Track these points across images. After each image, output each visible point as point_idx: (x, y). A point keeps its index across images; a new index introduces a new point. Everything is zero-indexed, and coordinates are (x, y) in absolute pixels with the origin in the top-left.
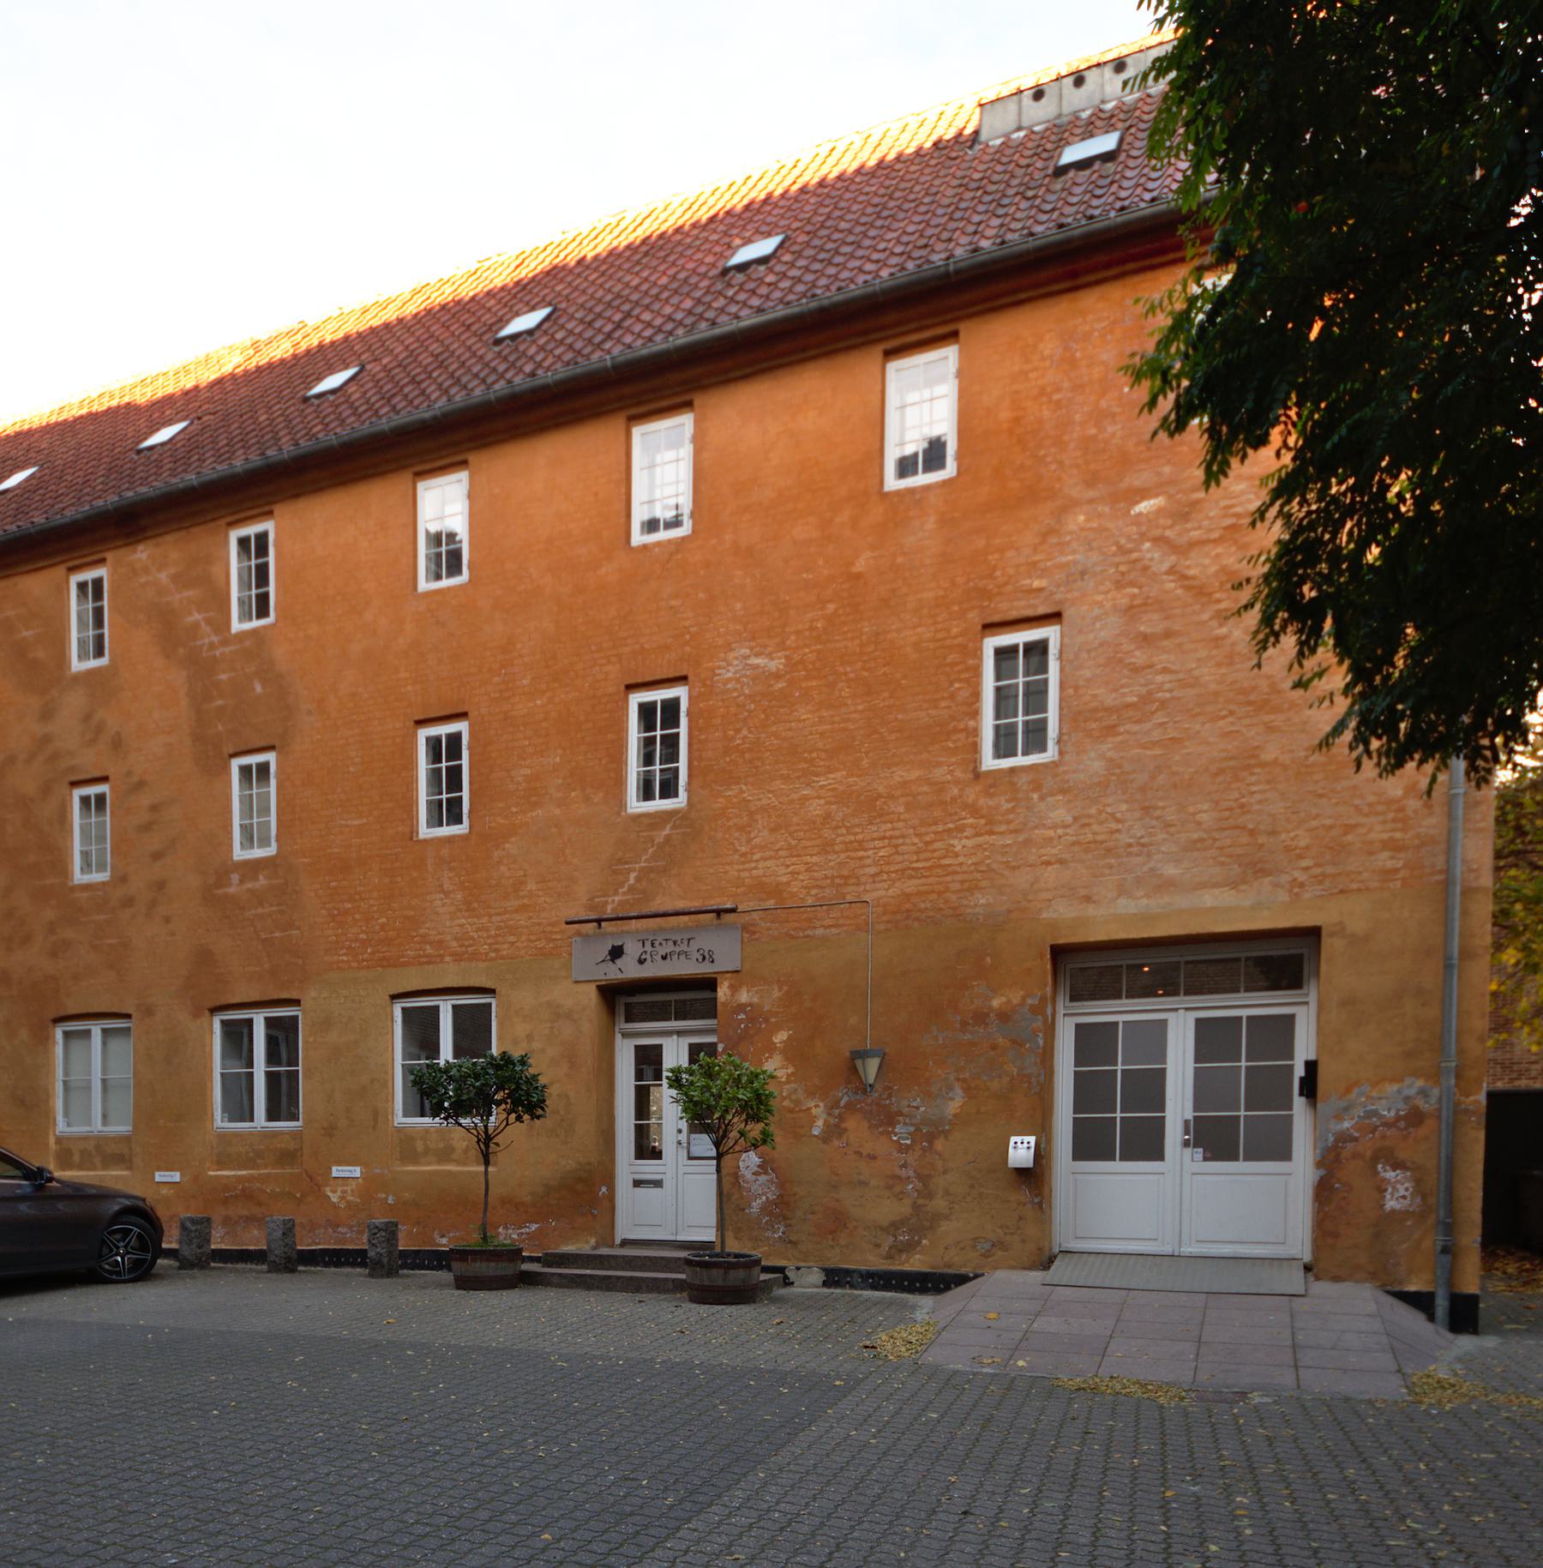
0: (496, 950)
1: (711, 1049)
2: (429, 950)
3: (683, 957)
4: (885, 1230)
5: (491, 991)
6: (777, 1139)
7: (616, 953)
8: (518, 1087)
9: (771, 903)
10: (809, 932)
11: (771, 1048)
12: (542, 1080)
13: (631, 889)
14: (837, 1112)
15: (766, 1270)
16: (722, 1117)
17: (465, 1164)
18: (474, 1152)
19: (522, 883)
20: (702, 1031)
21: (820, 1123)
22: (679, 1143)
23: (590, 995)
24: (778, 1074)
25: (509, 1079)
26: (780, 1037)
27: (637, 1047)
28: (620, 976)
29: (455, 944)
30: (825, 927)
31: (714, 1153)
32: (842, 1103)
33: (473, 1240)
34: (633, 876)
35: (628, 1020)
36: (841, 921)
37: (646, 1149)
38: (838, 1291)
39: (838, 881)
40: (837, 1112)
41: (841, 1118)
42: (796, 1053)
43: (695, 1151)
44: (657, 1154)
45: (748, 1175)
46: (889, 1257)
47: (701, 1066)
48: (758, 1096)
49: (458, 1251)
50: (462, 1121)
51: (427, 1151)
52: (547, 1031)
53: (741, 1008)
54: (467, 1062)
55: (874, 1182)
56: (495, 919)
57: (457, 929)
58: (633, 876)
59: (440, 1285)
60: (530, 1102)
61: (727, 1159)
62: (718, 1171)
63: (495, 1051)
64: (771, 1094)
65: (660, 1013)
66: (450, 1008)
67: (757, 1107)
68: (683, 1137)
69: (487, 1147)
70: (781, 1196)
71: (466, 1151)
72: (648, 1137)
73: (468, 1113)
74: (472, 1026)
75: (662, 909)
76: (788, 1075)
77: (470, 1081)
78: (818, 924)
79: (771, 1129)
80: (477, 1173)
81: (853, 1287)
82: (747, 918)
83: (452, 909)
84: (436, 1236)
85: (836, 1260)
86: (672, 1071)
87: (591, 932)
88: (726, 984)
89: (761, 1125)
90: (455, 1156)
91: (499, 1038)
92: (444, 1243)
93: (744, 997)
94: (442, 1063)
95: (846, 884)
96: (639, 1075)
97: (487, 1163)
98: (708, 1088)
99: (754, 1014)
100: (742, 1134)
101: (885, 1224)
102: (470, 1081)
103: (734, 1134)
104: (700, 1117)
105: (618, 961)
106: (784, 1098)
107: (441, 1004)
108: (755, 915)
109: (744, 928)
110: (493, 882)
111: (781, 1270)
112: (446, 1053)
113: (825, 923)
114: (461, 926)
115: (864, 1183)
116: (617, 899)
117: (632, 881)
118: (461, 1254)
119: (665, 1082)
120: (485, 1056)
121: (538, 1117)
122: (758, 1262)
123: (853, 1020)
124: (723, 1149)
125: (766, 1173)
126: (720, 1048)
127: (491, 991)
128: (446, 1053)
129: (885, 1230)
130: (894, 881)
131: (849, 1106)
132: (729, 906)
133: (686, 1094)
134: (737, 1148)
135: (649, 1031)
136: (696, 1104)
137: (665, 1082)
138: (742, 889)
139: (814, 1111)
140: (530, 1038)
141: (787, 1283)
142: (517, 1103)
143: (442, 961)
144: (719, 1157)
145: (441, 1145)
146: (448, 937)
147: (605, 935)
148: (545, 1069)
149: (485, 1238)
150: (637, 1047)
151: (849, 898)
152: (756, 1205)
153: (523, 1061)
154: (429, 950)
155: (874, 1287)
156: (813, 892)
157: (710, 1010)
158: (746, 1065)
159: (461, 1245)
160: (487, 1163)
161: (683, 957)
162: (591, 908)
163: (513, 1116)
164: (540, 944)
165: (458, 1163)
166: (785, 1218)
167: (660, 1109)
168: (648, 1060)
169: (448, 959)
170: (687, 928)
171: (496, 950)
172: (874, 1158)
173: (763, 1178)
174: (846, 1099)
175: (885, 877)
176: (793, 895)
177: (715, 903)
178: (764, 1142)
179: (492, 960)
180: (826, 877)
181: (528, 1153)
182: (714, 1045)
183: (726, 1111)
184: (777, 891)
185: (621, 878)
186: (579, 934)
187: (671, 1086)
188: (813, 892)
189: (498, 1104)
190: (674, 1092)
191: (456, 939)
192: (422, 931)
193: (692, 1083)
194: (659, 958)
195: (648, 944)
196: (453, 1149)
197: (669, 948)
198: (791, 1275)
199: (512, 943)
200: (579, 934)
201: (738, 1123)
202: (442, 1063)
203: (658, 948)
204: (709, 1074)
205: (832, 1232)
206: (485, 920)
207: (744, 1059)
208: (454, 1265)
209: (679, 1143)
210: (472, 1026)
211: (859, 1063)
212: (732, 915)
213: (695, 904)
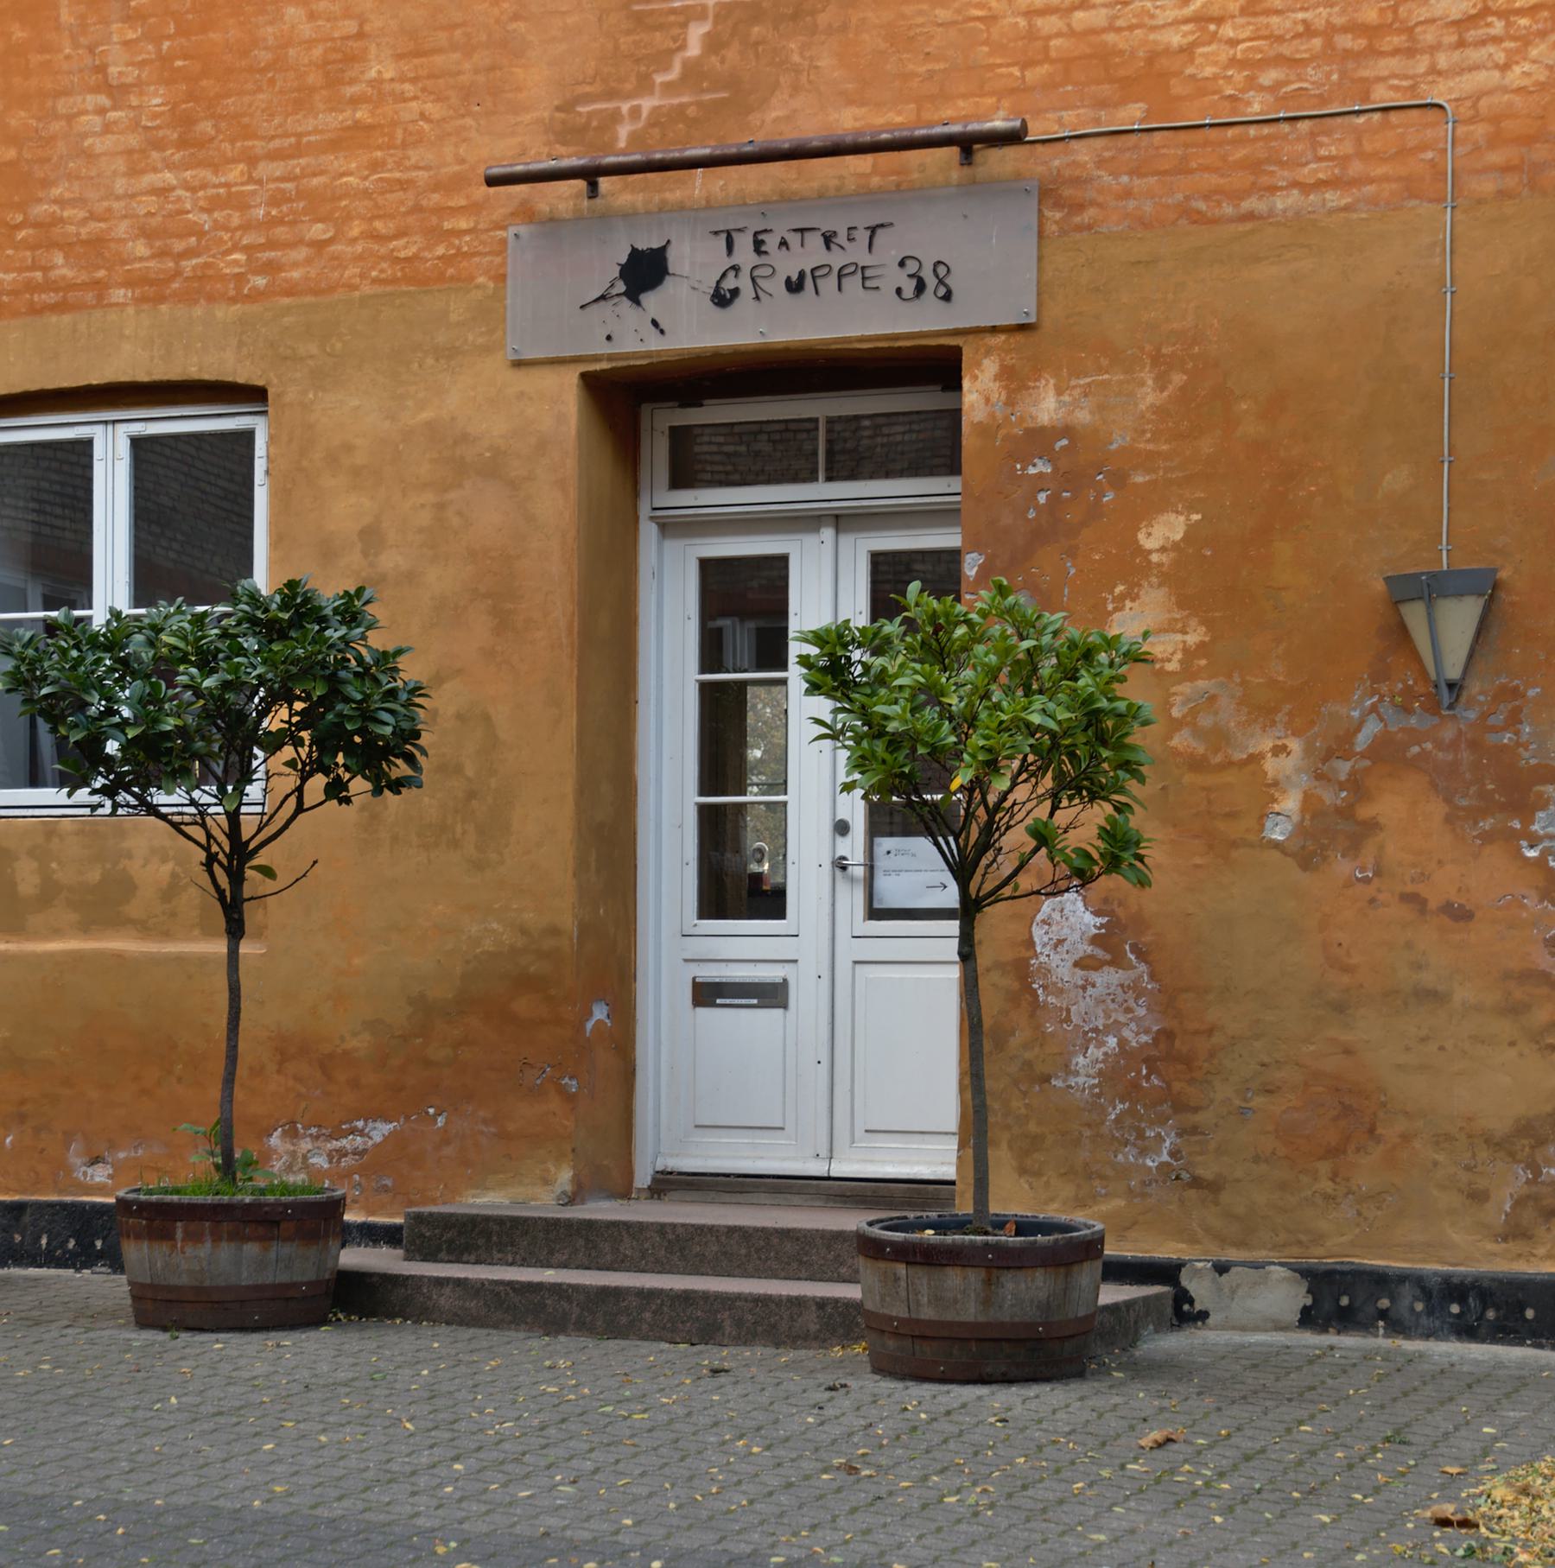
0: (271, 268)
1: (941, 571)
2: (62, 267)
3: (853, 284)
4: (1499, 1145)
5: (254, 395)
6: (1155, 854)
7: (645, 272)
8: (335, 692)
9: (1132, 114)
10: (1251, 204)
11: (1132, 568)
12: (410, 671)
13: (693, 74)
14: (1343, 768)
15: (1120, 1271)
16: (977, 786)
17: (167, 935)
18: (197, 898)
19: (351, 59)
20: (914, 511)
21: (1290, 803)
22: (840, 865)
23: (560, 404)
24: (1159, 647)
25: (309, 668)
26: (1162, 533)
27: (706, 565)
28: (655, 344)
29: (141, 249)
30: (1305, 188)
31: (950, 897)
32: (1362, 740)
33: (189, 1172)
34: (696, 34)
35: (680, 480)
36: (1356, 168)
37: (738, 885)
38: (1350, 1341)
39: (1345, 41)
40: (1343, 768)
41: (1357, 787)
42: (1213, 583)
43: (892, 892)
44: (767, 900)
45: (1061, 967)
46: (1514, 1232)
47: (911, 625)
48: (1094, 718)
49: (144, 1207)
50: (159, 798)
51: (49, 894)
52: (425, 518)
53: (1038, 440)
54: (175, 617)
55: (1463, 994)
56: (265, 169)
57: (149, 203)
58: (696, 34)
59: (88, 1315)
60: (370, 739)
61: (993, 918)
62: (967, 954)
63: (262, 578)
64: (1133, 712)
65: (780, 456)
66: (124, 449)
67: (1090, 753)
68: (853, 847)
69: (237, 878)
70: (1166, 1035)
71: (170, 892)
72: (738, 849)
73: (178, 775)
74: (194, 504)
75: (787, 136)
76: (1189, 654)
77: (187, 673)
78: (1282, 176)
79: (1136, 821)
80: (203, 961)
81: (1397, 1327)
82: (1055, 160)
83: (133, 140)
84: (75, 1158)
85: (1346, 1245)
86: (818, 638)
87: (565, 208)
88: (990, 366)
89: (1100, 813)
90: (134, 909)
91: (277, 540)
92: (99, 1184)
93: (1047, 407)
94: (98, 617)
95: (1373, 52)
96: (712, 653)
97: (235, 930)
98: (931, 694)
99: (1077, 460)
100: (1042, 837)
101: (1500, 1126)
102: (187, 673)
103: (1015, 839)
104: (904, 794)
105: (650, 299)
106: (1176, 725)
107: (97, 433)
108: (1083, 153)
109: (1048, 193)
110: (264, 56)
111: (1166, 1273)
112: (111, 587)
113: (1308, 173)
114: (163, 192)
115: (1432, 997)
116: (647, 104)
117: (694, 50)
118: (159, 1218)
119: (795, 675)
120: (233, 599)
121: (397, 786)
122: (1091, 1247)
123: (1396, 479)
124: (984, 882)
125: (1117, 961)
126: (971, 566)
127: (254, 395)
128: (111, 587)
129: (1499, 1145)
130: (1526, 41)
131: (1386, 753)
132: (998, 124)
133: (864, 713)
134: (1026, 882)
135: (738, 516)
136: (894, 743)
137: (795, 675)
138: (1034, 75)
139: (1271, 766)
140: (371, 538)
141: (1184, 1313)
142: (328, 743)
143: (101, 302)
144: (968, 911)
145: (95, 875)
146: (122, 229)
147: (606, 218)
148: (415, 634)
149: (228, 1168)
150: (706, 565)
151: (1382, 95)
152: (1087, 1064)
153: (350, 613)
154: (62, 267)
155: (1467, 1331)
156: (1269, 77)
157: (939, 448)
158: (1055, 618)
159: (156, 1186)
160: (235, 930)
161: (853, 284)
162: (567, 134)
163: (318, 782)
164: (406, 248)
165: (144, 928)
166: (1180, 1106)
167: (780, 757)
168: (744, 606)
169: (119, 294)
170: (867, 196)
171: (271, 268)
172: (1460, 915)
173: (1108, 978)
174: (1372, 728)
175: (1498, 27)
176: (1203, 87)
177: (956, 116)
178: (1113, 863)
179: (256, 296)
180: (1309, 31)
181: (367, 897)
182: (952, 557)
183: (992, 766)
184: (1152, 73)
185: (660, 40)
186: (526, 213)
187: (814, 688)
188: (1269, 77)
189: (273, 743)
190: (823, 706)
191: (147, 234)
192: (41, 210)
193: (882, 679)
194: (777, 286)
195: (744, 243)
196: (128, 887)
197: (811, 254)
198: (1199, 1288)
199: (320, 245)
200: (526, 213)
201: (1028, 801)
202: (98, 617)
203: (776, 256)
204: (938, 650)
205: (1333, 1152)
206: (235, 173)
207: (1048, 602)
208: (133, 1251)
209: (840, 865)
210: (194, 504)
211: (1414, 615)
212: (1011, 153)
213: (892, 119)
